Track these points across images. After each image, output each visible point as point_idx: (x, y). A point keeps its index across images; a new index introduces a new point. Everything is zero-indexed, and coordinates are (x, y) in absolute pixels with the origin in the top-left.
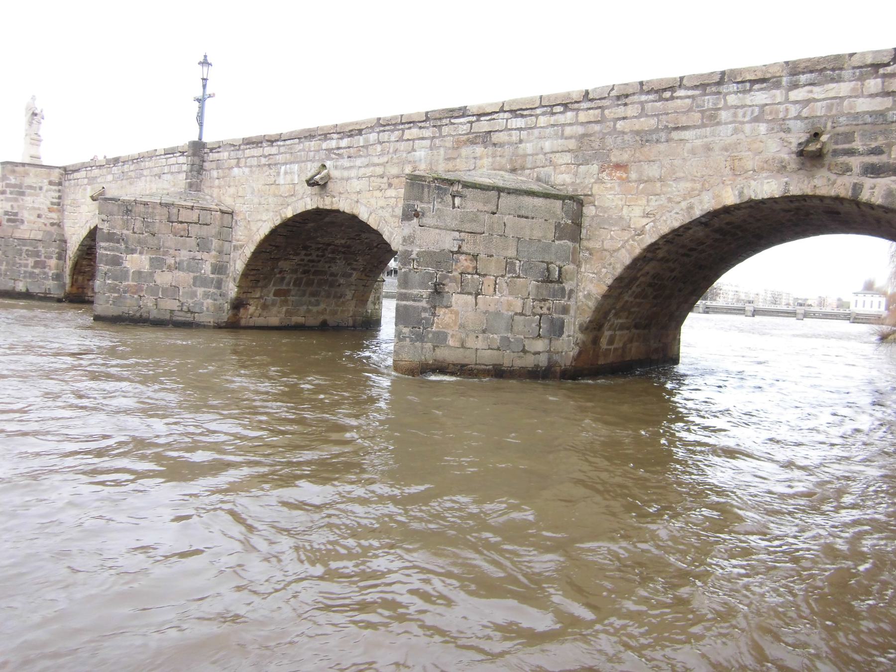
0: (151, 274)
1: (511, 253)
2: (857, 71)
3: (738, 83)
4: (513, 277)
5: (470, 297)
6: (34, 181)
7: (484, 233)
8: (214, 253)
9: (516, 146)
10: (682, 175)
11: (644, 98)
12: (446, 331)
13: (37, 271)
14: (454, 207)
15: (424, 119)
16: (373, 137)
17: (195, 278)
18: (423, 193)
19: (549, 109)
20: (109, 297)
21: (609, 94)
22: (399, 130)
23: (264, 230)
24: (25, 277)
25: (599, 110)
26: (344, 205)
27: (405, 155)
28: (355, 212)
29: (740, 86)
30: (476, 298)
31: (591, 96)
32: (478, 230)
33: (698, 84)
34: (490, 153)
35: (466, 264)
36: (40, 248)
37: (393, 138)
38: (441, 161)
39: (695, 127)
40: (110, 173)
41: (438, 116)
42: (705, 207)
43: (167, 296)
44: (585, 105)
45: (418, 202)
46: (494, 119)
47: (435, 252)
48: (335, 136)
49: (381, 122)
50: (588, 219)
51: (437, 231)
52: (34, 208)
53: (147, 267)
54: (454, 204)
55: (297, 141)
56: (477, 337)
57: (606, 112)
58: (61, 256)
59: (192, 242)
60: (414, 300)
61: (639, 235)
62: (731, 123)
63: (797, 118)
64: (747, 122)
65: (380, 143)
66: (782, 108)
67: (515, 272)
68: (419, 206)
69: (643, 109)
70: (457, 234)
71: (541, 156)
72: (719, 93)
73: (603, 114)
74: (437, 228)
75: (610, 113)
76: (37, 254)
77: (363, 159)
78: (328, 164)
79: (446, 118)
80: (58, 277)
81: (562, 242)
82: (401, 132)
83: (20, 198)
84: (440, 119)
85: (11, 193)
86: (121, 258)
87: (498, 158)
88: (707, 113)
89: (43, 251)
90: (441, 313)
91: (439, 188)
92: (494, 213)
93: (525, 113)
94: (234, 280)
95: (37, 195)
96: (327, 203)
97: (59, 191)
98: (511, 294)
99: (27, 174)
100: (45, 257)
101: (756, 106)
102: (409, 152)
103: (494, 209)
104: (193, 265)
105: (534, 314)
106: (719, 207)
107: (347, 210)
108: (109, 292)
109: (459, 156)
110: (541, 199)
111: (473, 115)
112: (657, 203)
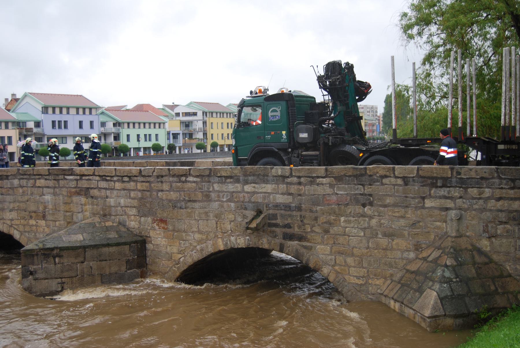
2: (275, 178)
3: (219, 177)
7: (78, 276)
9: (105, 199)
11: (171, 179)
14: (55, 264)
15: (47, 173)
16: (16, 182)
19: (120, 178)
21: (152, 173)
22: (32, 179)
25: (147, 184)
27: (38, 197)
31: (143, 174)
32: (74, 275)
33: (198, 174)
34: (90, 202)
37: (29, 185)
38: (61, 204)
39: (199, 201)
41: (56, 173)
42: (209, 250)
44: (140, 179)
46: (90, 180)
49: (20, 172)
50: (150, 252)
51: (46, 281)
54: (55, 262)
57: (152, 185)
61: (177, 264)
63: (250, 202)
65: (22, 187)
66: (241, 195)
68: (32, 268)
69: (171, 186)
70: (59, 280)
71: (119, 208)
72: (209, 182)
73: (150, 186)
74: (46, 279)
75: (155, 186)
77: (11, 196)
79: (62, 175)
82: (34, 180)
84: (57, 175)
87: (95, 206)
88: (205, 193)
91: (44, 254)
92: (83, 262)
93: (108, 178)
101: (229, 192)
102: (41, 196)
103: (82, 259)
106: (216, 250)
109: (72, 201)
110: (114, 247)
111: (77, 175)
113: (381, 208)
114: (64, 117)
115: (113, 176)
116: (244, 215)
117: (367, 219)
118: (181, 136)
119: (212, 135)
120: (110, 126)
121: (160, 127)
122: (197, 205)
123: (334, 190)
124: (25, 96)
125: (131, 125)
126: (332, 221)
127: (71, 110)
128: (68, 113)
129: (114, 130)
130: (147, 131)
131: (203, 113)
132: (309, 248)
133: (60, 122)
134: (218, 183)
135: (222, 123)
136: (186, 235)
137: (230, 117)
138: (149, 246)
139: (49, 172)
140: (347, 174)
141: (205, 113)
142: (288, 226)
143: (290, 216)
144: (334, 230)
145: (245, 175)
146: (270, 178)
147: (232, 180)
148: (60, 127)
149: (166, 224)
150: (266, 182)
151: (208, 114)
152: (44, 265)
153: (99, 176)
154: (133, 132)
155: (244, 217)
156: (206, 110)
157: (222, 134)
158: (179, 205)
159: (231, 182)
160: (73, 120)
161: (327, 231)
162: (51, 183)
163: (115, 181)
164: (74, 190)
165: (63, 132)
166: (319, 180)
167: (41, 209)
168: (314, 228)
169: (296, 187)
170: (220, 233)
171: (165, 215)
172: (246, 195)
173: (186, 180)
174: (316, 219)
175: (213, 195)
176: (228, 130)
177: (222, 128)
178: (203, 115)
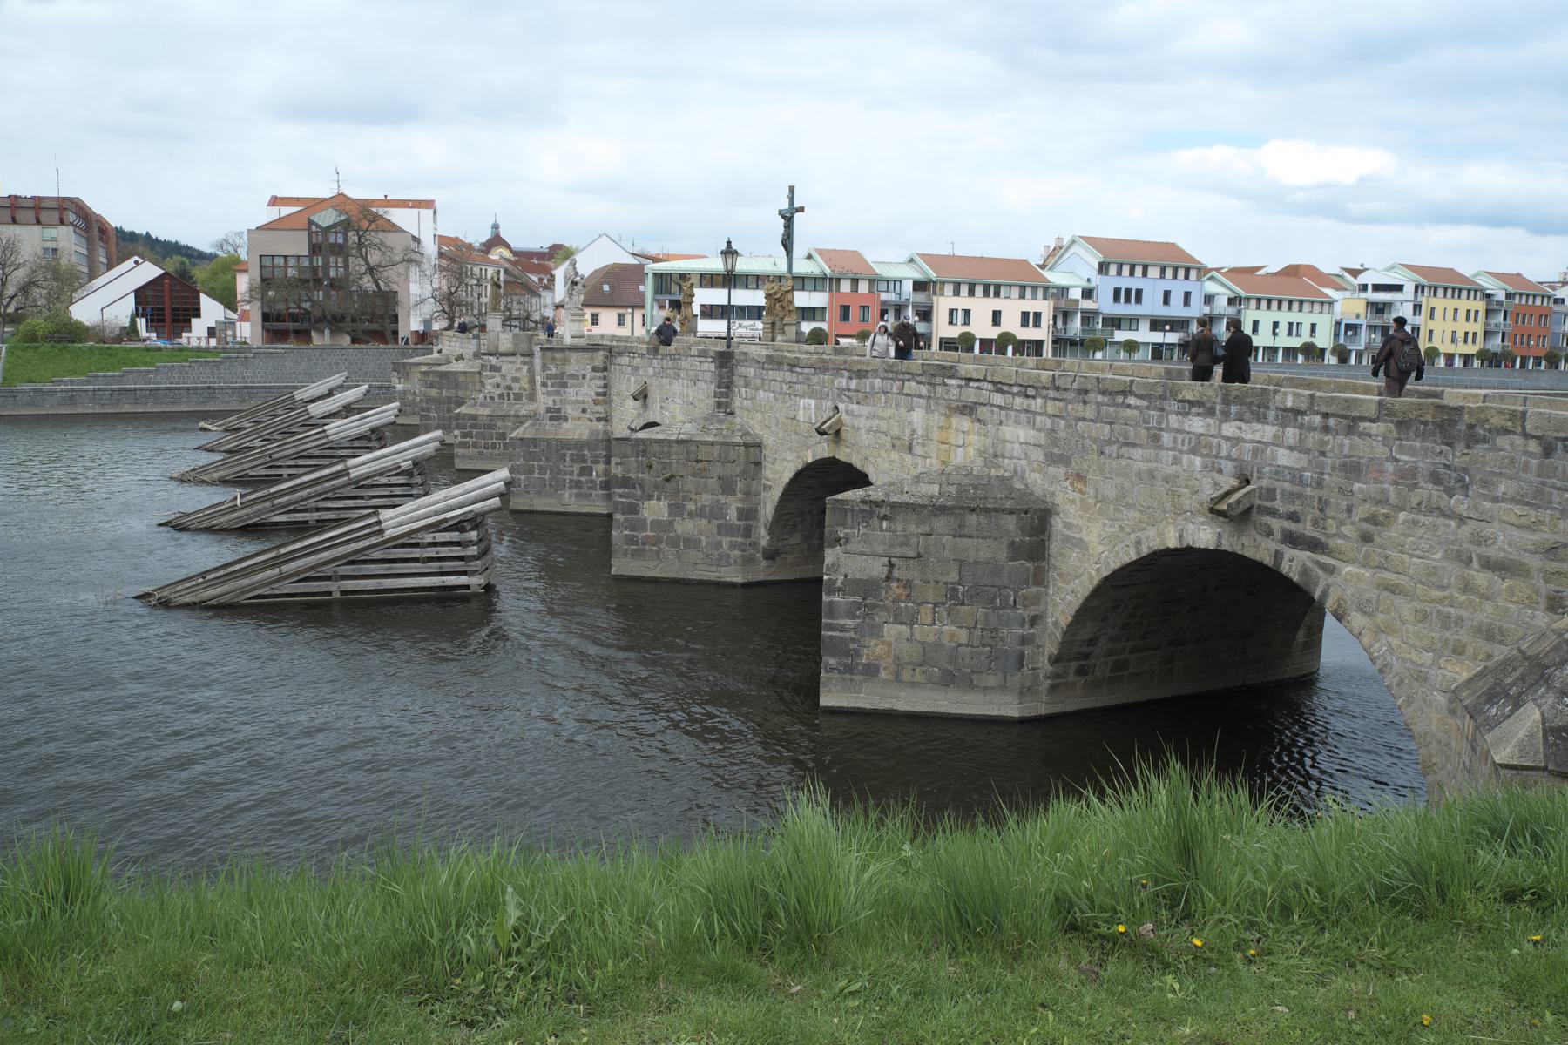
0: (671, 523)
1: (953, 577)
4: (954, 605)
5: (904, 627)
8: (739, 495)
10: (1131, 501)
11: (1100, 398)
12: (877, 662)
13: (583, 479)
14: (881, 530)
15: (920, 372)
17: (719, 526)
18: (846, 518)
20: (627, 550)
23: (788, 476)
24: (570, 487)
25: (1061, 404)
29: (1180, 405)
30: (911, 629)
35: (898, 591)
36: (586, 452)
38: (935, 428)
39: (1141, 446)
43: (690, 548)
44: (1052, 393)
45: (841, 528)
47: (861, 580)
48: (846, 373)
51: (864, 557)
52: (578, 402)
53: (666, 515)
55: (813, 370)
56: (914, 670)
59: (713, 482)
60: (841, 631)
62: (1171, 449)
64: (1185, 453)
67: (958, 598)
69: (1099, 412)
72: (1162, 410)
76: (583, 459)
78: (841, 406)
83: (562, 390)
85: (552, 385)
86: (638, 505)
90: (872, 644)
93: (1005, 388)
94: (765, 526)
95: (580, 386)
96: (842, 455)
97: (605, 378)
98: (953, 623)
99: (566, 361)
100: (592, 462)
101: (1194, 434)
104: (716, 512)
105: (984, 645)
106: (1162, 548)
107: (858, 465)
108: (627, 544)
111: (961, 379)
112: (1111, 530)
113: (1485, 503)
115: (1011, 385)
117: (1453, 523)
122: (1137, 453)
123: (1391, 451)
126: (1381, 518)
127: (1150, 269)
128: (1145, 274)
129: (1231, 311)
130: (1295, 316)
131: (1416, 287)
132: (1330, 570)
133: (1128, 291)
134: (1177, 413)
135: (1456, 310)
136: (1115, 509)
137: (1475, 299)
138: (1057, 524)
139: (923, 368)
140: (1421, 419)
141: (1419, 288)
142: (1293, 517)
143: (1300, 496)
145: (1227, 401)
146: (1271, 414)
147: (1201, 410)
148: (1128, 300)
150: (1262, 419)
151: (1426, 290)
152: (862, 531)
153: (992, 382)
154: (1266, 317)
155: (1216, 485)
156: (1424, 281)
157: (1454, 332)
158: (1107, 449)
159: (1198, 414)
160: (1152, 288)
161: (1366, 538)
162: (924, 390)
163: (1014, 395)
164: (954, 405)
165: (1132, 309)
166: (1363, 426)
167: (907, 433)
168: (1343, 529)
169: (1317, 435)
170: (1172, 515)
171: (1085, 466)
172: (1223, 442)
173: (1123, 402)
174: (1349, 510)
175: (1166, 438)
176: (1467, 324)
177: (1455, 319)
178: (1416, 291)
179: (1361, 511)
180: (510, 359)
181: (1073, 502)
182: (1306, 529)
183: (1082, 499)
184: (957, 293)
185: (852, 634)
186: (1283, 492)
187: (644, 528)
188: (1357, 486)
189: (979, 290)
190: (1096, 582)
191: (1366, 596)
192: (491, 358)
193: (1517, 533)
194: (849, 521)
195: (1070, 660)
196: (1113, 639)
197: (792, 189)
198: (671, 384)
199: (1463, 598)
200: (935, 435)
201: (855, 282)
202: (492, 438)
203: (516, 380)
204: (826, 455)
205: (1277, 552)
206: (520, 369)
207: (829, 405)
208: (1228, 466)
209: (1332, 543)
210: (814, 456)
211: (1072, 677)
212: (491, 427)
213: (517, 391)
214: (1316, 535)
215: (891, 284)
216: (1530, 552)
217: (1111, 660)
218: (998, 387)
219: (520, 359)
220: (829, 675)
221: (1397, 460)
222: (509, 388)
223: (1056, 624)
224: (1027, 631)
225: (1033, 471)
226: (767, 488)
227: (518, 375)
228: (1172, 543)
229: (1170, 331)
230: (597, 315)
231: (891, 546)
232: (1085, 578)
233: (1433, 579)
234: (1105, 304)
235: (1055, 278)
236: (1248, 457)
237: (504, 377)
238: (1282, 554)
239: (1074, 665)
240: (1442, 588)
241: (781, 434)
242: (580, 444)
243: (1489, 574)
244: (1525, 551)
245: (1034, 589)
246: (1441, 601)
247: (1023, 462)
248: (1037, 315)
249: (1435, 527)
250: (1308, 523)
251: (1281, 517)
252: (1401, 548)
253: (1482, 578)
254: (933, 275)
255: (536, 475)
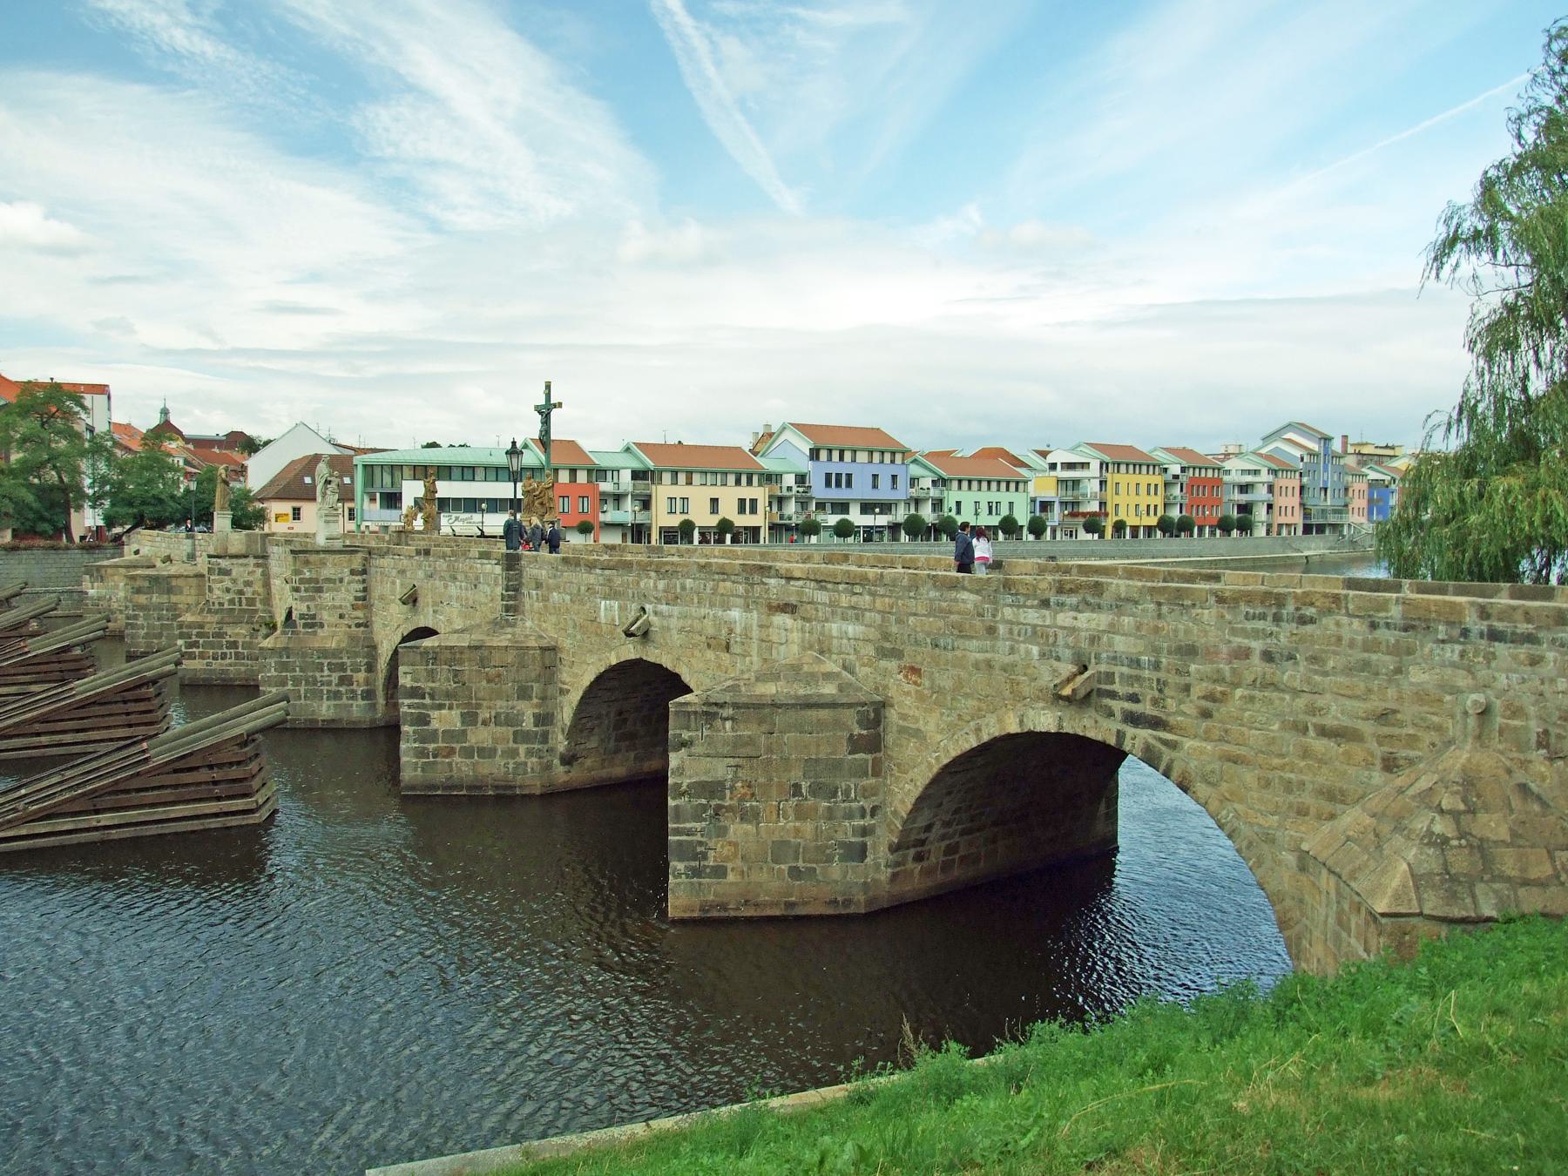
0: (464, 732)
6: (333, 571)
8: (535, 701)
16: (689, 583)
17: (515, 733)
20: (416, 763)
23: (588, 678)
24: (328, 699)
26: (667, 662)
28: (677, 671)
35: (743, 791)
36: (345, 660)
38: (755, 627)
40: (420, 567)
52: (335, 607)
53: (459, 724)
58: (371, 668)
62: (1008, 639)
67: (802, 795)
70: (732, 761)
78: (648, 607)
80: (369, 695)
81: (857, 756)
83: (317, 595)
85: (306, 590)
89: (348, 662)
93: (829, 586)
94: (563, 730)
97: (364, 581)
98: (798, 818)
114: (843, 469)
116: (1055, 671)
117: (1287, 697)
118: (1057, 506)
119: (1117, 505)
120: (926, 483)
121: (1017, 490)
122: (975, 643)
124: (784, 429)
125: (965, 484)
126: (1218, 695)
128: (854, 460)
129: (934, 493)
130: (994, 496)
131: (1101, 464)
132: (1173, 745)
133: (839, 476)
138: (892, 715)
141: (1104, 465)
142: (1134, 698)
143: (1138, 679)
144: (1222, 711)
148: (838, 485)
149: (920, 676)
151: (1110, 466)
153: (816, 581)
154: (968, 497)
156: (1107, 459)
161: (1206, 714)
164: (775, 603)
167: (724, 632)
168: (1182, 707)
174: (1187, 689)
175: (1002, 629)
177: (1137, 494)
179: (1198, 690)
180: (241, 561)
181: (908, 693)
182: (1146, 708)
183: (917, 691)
184: (675, 482)
185: (698, 838)
186: (1122, 674)
187: (435, 741)
188: (1193, 667)
189: (696, 478)
190: (935, 770)
191: (1209, 768)
192: (219, 560)
193: (1348, 702)
194: (693, 725)
195: (908, 848)
196: (947, 824)
197: (548, 386)
198: (446, 587)
199: (1302, 764)
200: (755, 633)
201: (573, 472)
202: (221, 648)
203: (248, 584)
204: (632, 656)
205: (1118, 731)
206: (253, 572)
207: (635, 606)
208: (1068, 653)
209: (1172, 720)
210: (618, 657)
211: (910, 865)
212: (220, 635)
213: (249, 595)
214: (1155, 713)
215: (609, 474)
216: (1363, 719)
217: (944, 844)
218: (820, 583)
219: (252, 561)
220: (679, 880)
221: (1230, 642)
222: (241, 592)
223: (895, 813)
224: (868, 821)
225: (864, 665)
226: (563, 692)
227: (251, 579)
228: (1014, 728)
229: (881, 513)
230: (299, 509)
231: (735, 746)
232: (923, 767)
233: (1272, 748)
234: (819, 491)
235: (767, 464)
236: (1084, 645)
237: (234, 581)
238: (1124, 734)
239: (912, 852)
240: (1281, 756)
241: (579, 637)
242: (336, 653)
243: (1325, 741)
244: (1357, 718)
245: (872, 781)
246: (1282, 768)
247: (852, 657)
248: (754, 502)
249: (1271, 702)
250: (1148, 703)
251: (1120, 699)
252: (1239, 720)
253: (1320, 745)
254: (651, 465)
255: (290, 687)
